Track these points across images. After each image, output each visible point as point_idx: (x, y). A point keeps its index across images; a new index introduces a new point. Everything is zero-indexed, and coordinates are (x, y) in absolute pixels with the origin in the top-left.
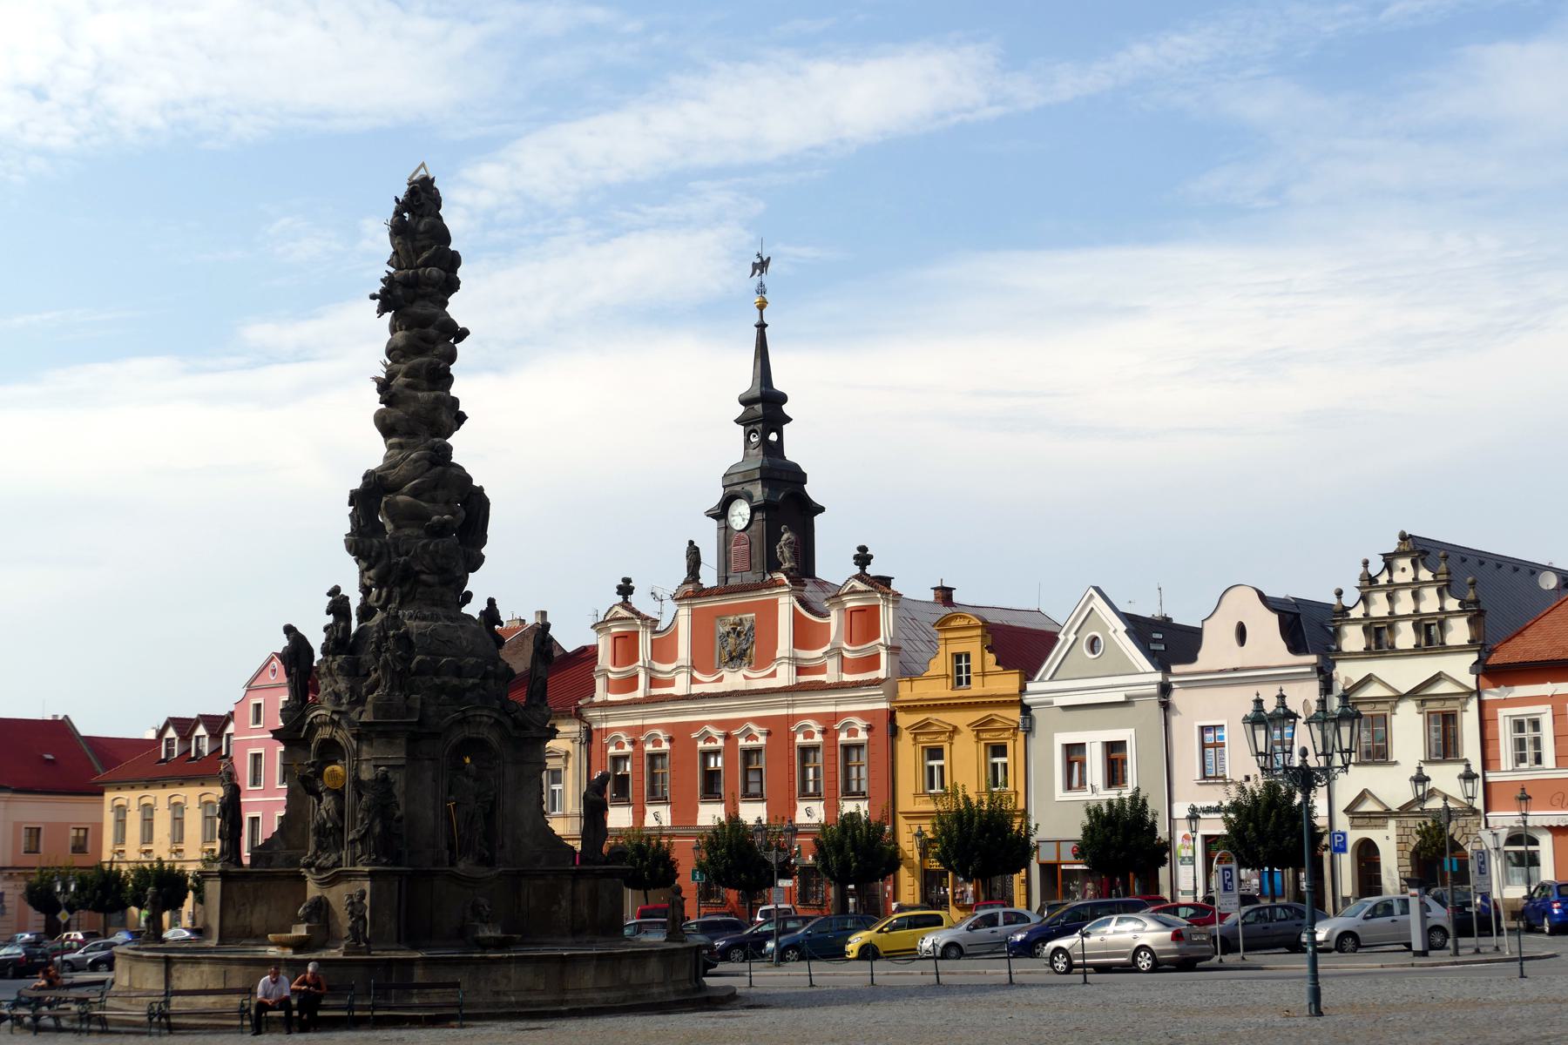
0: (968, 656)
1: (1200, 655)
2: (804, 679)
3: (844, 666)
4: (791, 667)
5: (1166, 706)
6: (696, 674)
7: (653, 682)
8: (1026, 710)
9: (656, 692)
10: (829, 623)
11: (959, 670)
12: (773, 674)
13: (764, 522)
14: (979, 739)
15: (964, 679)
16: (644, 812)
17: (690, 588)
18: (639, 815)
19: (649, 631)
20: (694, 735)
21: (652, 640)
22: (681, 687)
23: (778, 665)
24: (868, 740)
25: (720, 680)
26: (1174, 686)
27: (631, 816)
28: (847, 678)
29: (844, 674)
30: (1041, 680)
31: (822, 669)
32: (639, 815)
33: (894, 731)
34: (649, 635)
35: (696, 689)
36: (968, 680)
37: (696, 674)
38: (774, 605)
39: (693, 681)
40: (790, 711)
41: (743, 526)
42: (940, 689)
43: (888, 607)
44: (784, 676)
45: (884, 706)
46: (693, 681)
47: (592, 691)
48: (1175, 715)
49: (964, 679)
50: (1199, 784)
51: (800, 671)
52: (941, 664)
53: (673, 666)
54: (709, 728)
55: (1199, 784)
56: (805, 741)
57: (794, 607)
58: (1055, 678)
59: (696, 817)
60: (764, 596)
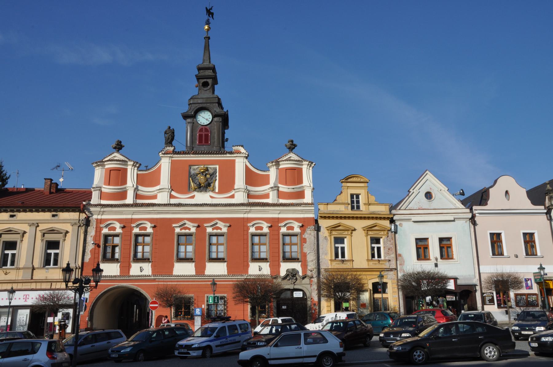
0: (358, 196)
1: (489, 202)
2: (252, 201)
3: (280, 195)
4: (245, 193)
5: (474, 224)
6: (173, 193)
7: (137, 196)
8: (392, 221)
9: (139, 201)
10: (268, 176)
11: (352, 202)
12: (232, 197)
13: (221, 123)
14: (367, 235)
15: (355, 206)
16: (129, 267)
17: (171, 149)
18: (125, 268)
19: (136, 168)
20: (174, 225)
21: (137, 174)
22: (162, 198)
23: (235, 192)
24: (301, 232)
25: (193, 197)
26: (477, 215)
27: (119, 269)
28: (282, 201)
29: (280, 199)
30: (400, 209)
31: (267, 196)
32: (125, 268)
33: (318, 229)
34: (136, 171)
35: (173, 201)
36: (358, 207)
37: (173, 193)
38: (232, 164)
39: (171, 197)
40: (246, 216)
41: (206, 124)
42: (345, 209)
43: (309, 169)
44: (240, 197)
45: (312, 216)
46: (171, 197)
47: (90, 199)
48: (477, 226)
49: (355, 206)
50: (492, 257)
51: (249, 196)
52: (345, 197)
53: (158, 187)
54: (186, 222)
55: (492, 257)
56: (256, 231)
57: (246, 165)
58: (406, 209)
59: (173, 270)
60: (227, 157)
